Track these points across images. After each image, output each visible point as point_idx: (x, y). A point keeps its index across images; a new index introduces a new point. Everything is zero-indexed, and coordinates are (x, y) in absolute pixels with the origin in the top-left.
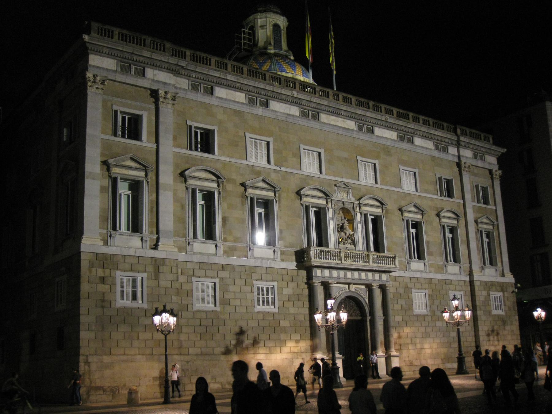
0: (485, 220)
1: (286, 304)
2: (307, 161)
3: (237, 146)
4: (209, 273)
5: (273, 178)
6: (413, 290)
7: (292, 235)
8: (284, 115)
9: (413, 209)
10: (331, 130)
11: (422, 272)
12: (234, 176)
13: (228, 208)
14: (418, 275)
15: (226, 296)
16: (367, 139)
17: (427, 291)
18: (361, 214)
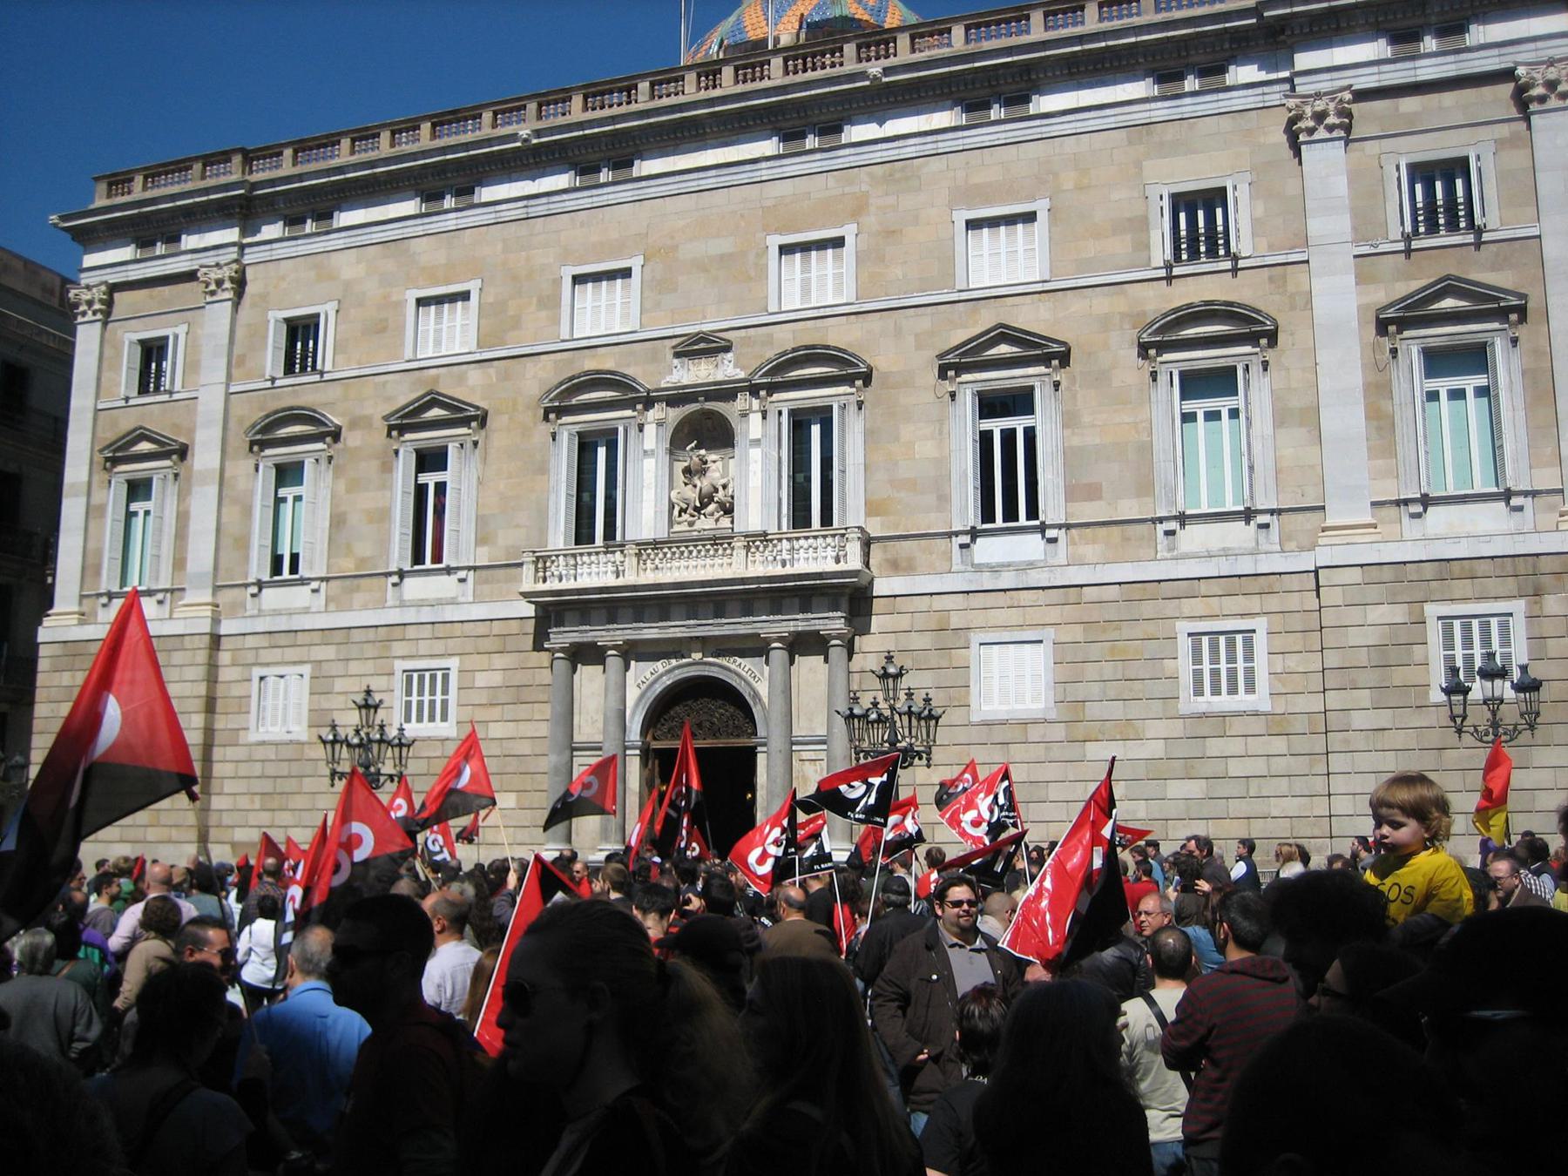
0: (1448, 303)
1: (480, 715)
2: (589, 304)
3: (384, 330)
4: (291, 654)
5: (471, 388)
6: (976, 638)
7: (517, 526)
8: (520, 204)
9: (1004, 349)
10: (673, 189)
11: (1031, 565)
12: (368, 411)
13: (348, 491)
14: (1007, 580)
15: (325, 705)
16: (815, 167)
17: (1049, 634)
18: (764, 418)
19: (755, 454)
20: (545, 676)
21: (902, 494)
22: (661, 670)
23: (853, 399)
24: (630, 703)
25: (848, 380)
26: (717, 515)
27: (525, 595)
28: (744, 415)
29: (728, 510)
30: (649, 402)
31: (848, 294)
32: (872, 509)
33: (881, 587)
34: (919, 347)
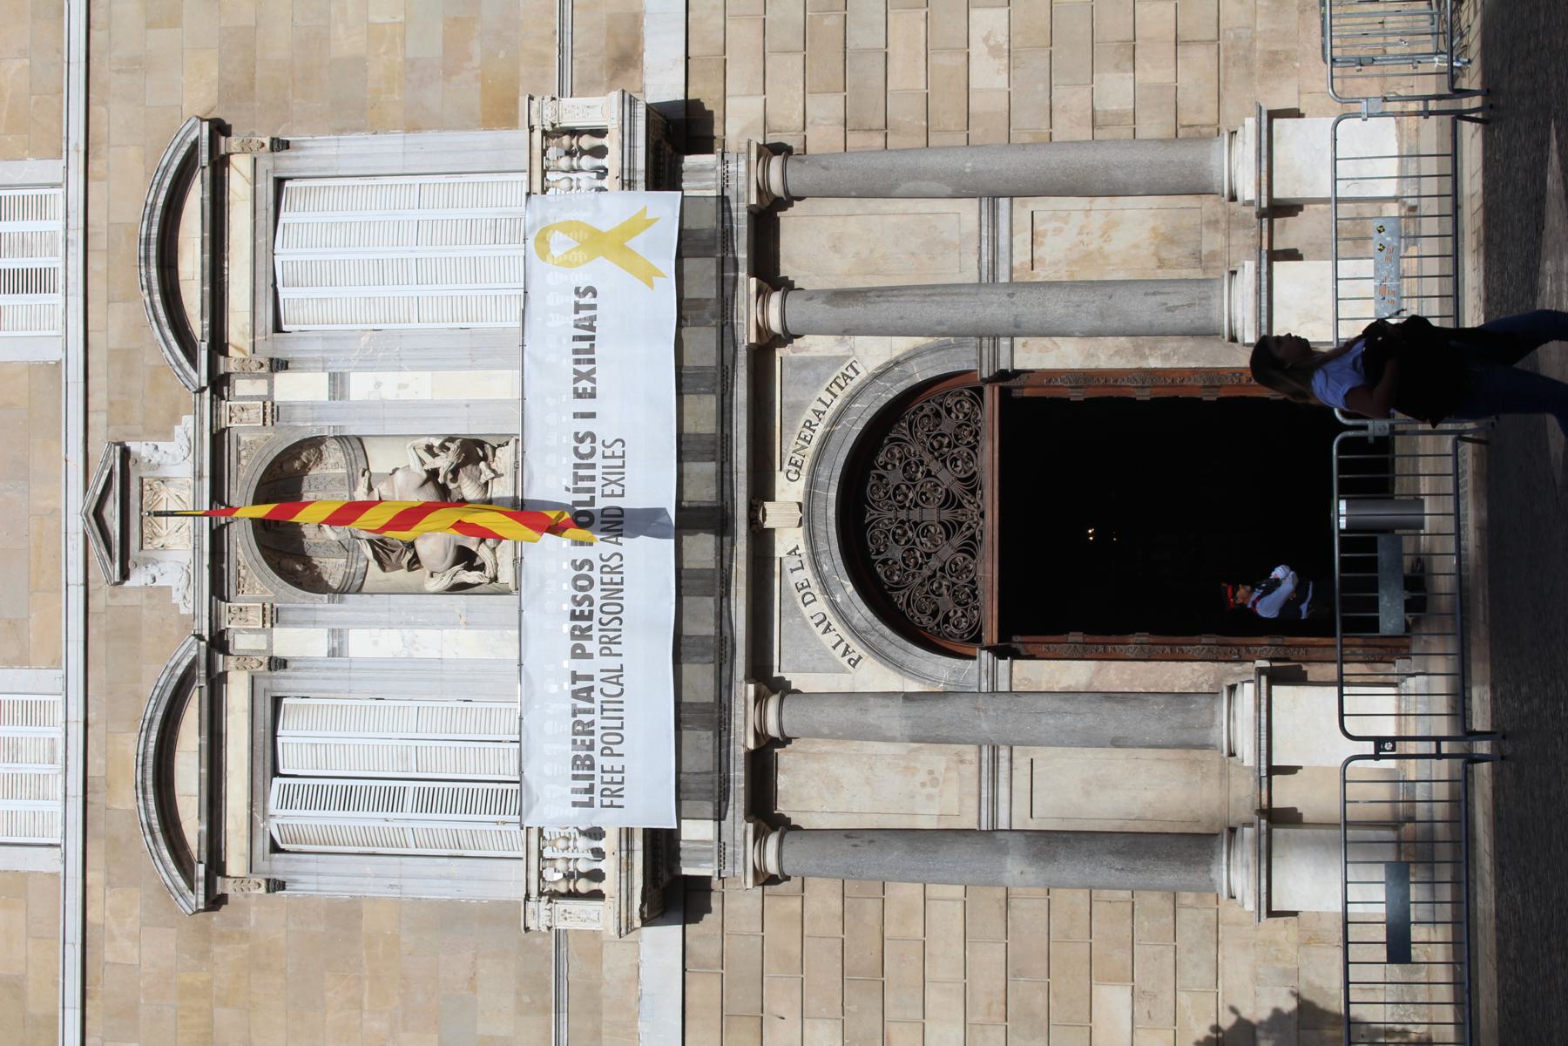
7: (472, 980)
19: (361, 386)
20: (823, 897)
21: (476, 48)
22: (821, 606)
23: (266, 162)
24: (894, 682)
25: (220, 164)
26: (487, 475)
27: (626, 928)
28: (273, 412)
29: (473, 451)
30: (218, 642)
31: (51, 169)
32: (500, 114)
33: (663, 83)
34: (174, 21)
